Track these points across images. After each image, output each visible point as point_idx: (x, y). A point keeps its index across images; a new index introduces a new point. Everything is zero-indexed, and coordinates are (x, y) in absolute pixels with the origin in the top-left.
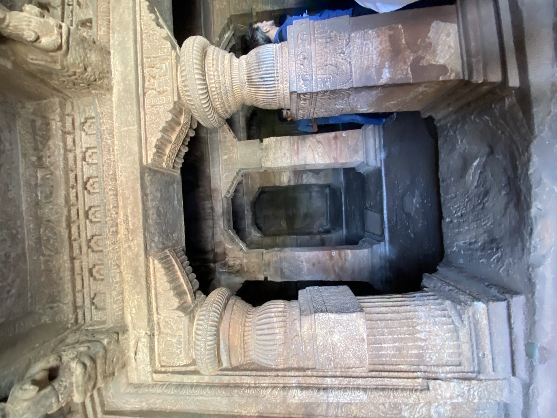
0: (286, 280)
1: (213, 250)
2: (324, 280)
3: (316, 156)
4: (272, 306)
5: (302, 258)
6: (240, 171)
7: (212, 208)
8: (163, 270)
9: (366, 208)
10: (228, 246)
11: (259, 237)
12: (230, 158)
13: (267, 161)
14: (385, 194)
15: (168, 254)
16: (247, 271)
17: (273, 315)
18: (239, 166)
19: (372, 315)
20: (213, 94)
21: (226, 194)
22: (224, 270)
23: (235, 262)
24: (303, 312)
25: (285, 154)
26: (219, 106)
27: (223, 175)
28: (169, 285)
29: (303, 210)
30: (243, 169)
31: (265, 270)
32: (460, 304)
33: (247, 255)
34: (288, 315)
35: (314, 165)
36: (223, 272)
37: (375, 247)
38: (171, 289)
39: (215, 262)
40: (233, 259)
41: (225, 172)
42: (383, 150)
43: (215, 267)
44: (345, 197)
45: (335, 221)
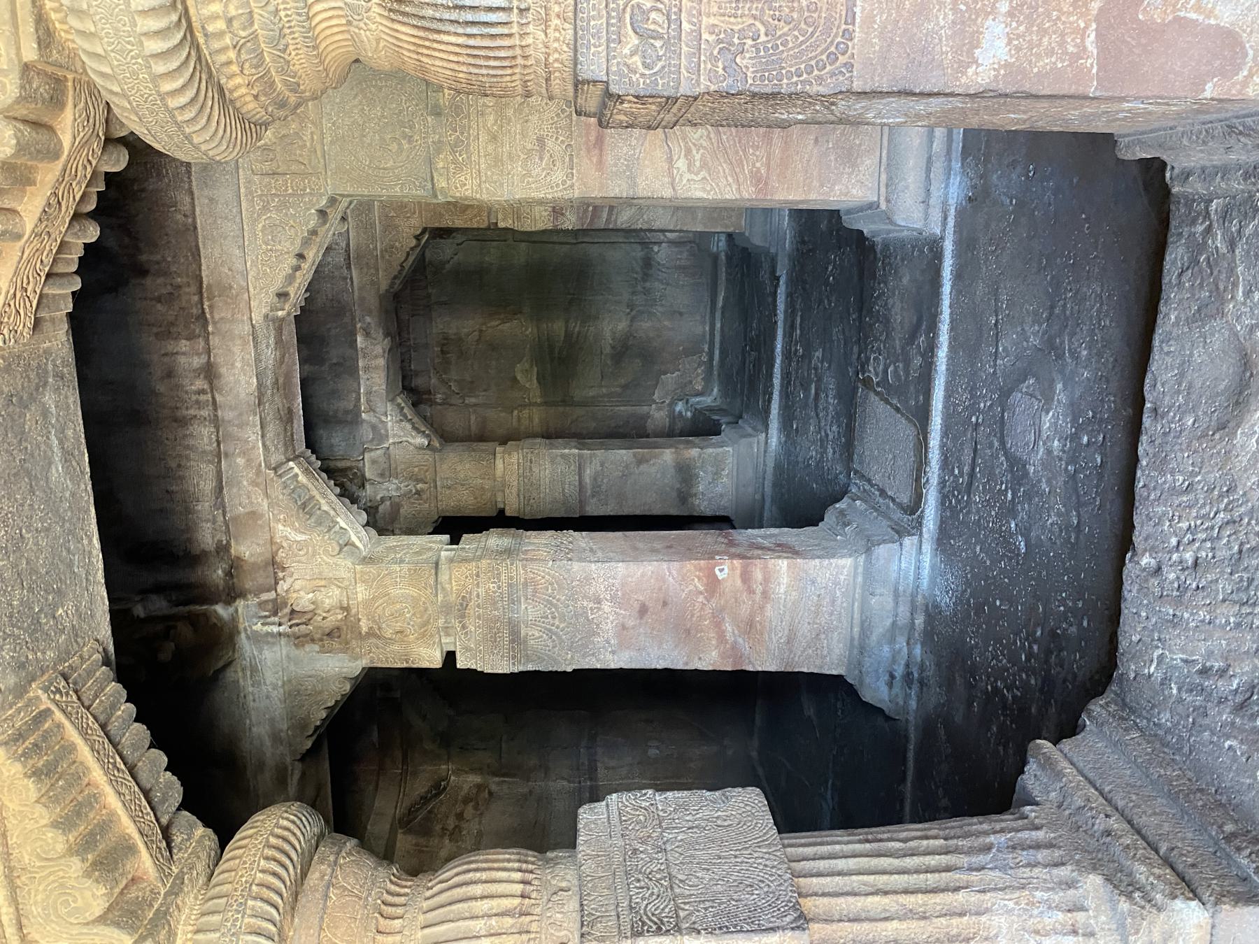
0: (530, 667)
1: (223, 549)
2: (680, 666)
3: (681, 164)
4: (478, 890)
5: (599, 587)
7: (210, 372)
8: (31, 783)
10: (288, 532)
11: (420, 448)
13: (459, 168)
14: (942, 354)
15: (45, 703)
16: (371, 634)
17: (479, 926)
19: (835, 926)
20: (216, 45)
22: (275, 629)
23: (320, 596)
24: (592, 924)
25: (541, 141)
26: (243, 90)
27: (254, 221)
28: (61, 838)
29: (611, 326)
31: (447, 630)
32: (1129, 896)
33: (372, 569)
34: (534, 927)
36: (272, 634)
37: (882, 551)
38: (71, 852)
39: (232, 594)
41: (265, 209)
42: (957, 165)
43: (234, 619)
44: (790, 295)
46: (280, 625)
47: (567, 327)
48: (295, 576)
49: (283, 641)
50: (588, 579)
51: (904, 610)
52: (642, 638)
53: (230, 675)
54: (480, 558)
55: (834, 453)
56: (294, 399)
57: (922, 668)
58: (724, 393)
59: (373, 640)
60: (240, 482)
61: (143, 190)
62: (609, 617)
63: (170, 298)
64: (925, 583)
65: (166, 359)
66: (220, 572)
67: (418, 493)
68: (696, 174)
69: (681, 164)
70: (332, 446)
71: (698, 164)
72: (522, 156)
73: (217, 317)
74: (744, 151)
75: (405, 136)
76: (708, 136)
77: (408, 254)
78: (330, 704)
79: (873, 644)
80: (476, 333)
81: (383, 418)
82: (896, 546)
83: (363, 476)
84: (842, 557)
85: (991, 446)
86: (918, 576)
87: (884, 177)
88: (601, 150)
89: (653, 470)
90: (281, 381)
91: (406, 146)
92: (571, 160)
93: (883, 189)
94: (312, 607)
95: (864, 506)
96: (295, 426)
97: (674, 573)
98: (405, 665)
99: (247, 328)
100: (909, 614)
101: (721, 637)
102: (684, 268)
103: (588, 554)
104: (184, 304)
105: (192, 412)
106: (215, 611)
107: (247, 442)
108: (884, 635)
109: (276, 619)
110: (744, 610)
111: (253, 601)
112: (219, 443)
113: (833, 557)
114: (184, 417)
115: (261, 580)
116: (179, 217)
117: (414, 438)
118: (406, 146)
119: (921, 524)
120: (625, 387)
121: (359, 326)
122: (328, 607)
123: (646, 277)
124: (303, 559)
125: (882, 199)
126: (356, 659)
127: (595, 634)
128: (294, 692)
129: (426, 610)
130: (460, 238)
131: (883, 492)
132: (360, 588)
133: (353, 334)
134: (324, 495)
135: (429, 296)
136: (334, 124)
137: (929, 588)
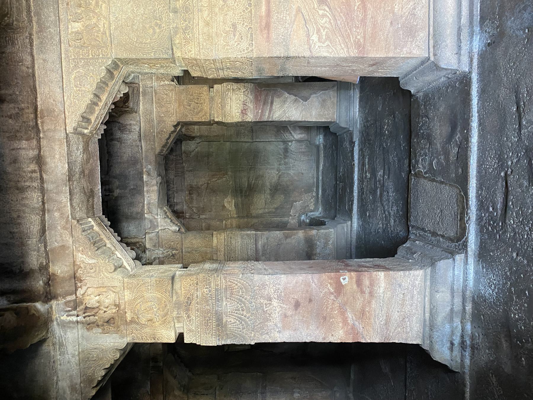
0: (229, 342)
1: (44, 268)
2: (320, 340)
3: (315, 38)
5: (270, 290)
6: (116, 65)
7: (39, 160)
9: (418, 175)
10: (84, 258)
11: (175, 232)
12: (89, 29)
13: (187, 41)
14: (474, 139)
16: (132, 322)
18: (115, 53)
21: (79, 126)
25: (234, 26)
29: (271, 174)
30: (126, 62)
33: (134, 281)
35: (307, 60)
36: (72, 322)
37: (442, 264)
39: (48, 297)
40: (97, 292)
41: (76, 66)
42: (477, 29)
43: (49, 312)
44: (361, 150)
45: (336, 202)
46: (78, 316)
47: (248, 181)
48: (88, 285)
49: (80, 326)
50: (263, 286)
51: (458, 301)
52: (297, 322)
53: (45, 348)
54: (198, 273)
55: (395, 222)
56: (95, 185)
57: (472, 338)
58: (325, 210)
59: (134, 325)
60: (56, 227)
61: (3, 53)
62: (277, 308)
63: (16, 116)
64: (471, 283)
65: (14, 152)
66: (41, 282)
67: (173, 255)
68: (324, 43)
69: (315, 38)
70: (129, 231)
71: (324, 37)
72: (224, 35)
73: (45, 128)
74: (350, 29)
75: (157, 24)
76: (330, 22)
77: (170, 136)
78: (107, 367)
79: (439, 324)
80: (206, 185)
81: (156, 217)
82: (451, 261)
83: (145, 247)
84: (416, 269)
85: (521, 186)
86: (465, 280)
87: (431, 42)
88: (268, 30)
89: (293, 241)
90: (87, 172)
91: (158, 31)
92: (252, 36)
93: (431, 50)
94: (98, 305)
95: (422, 244)
96: (96, 200)
97: (316, 280)
98: (153, 341)
99: (63, 135)
100: (461, 304)
101: (345, 321)
102: (304, 152)
103: (263, 271)
104: (25, 120)
105: (27, 184)
106: (35, 306)
107: (61, 203)
108: (445, 318)
109: (75, 312)
110: (359, 305)
111: (61, 301)
112: (43, 203)
113: (411, 269)
114: (23, 187)
115: (67, 288)
116: (24, 68)
117: (171, 227)
118: (158, 31)
119: (466, 246)
120: (276, 209)
121: (144, 170)
122: (107, 305)
123: (286, 157)
124: (93, 275)
125: (431, 54)
126: (123, 338)
127: (268, 320)
128: (85, 359)
129: (166, 306)
130: (198, 140)
131: (434, 234)
132: (127, 293)
133: (141, 173)
134: (109, 238)
135: (183, 167)
136: (116, 18)
137: (474, 286)
